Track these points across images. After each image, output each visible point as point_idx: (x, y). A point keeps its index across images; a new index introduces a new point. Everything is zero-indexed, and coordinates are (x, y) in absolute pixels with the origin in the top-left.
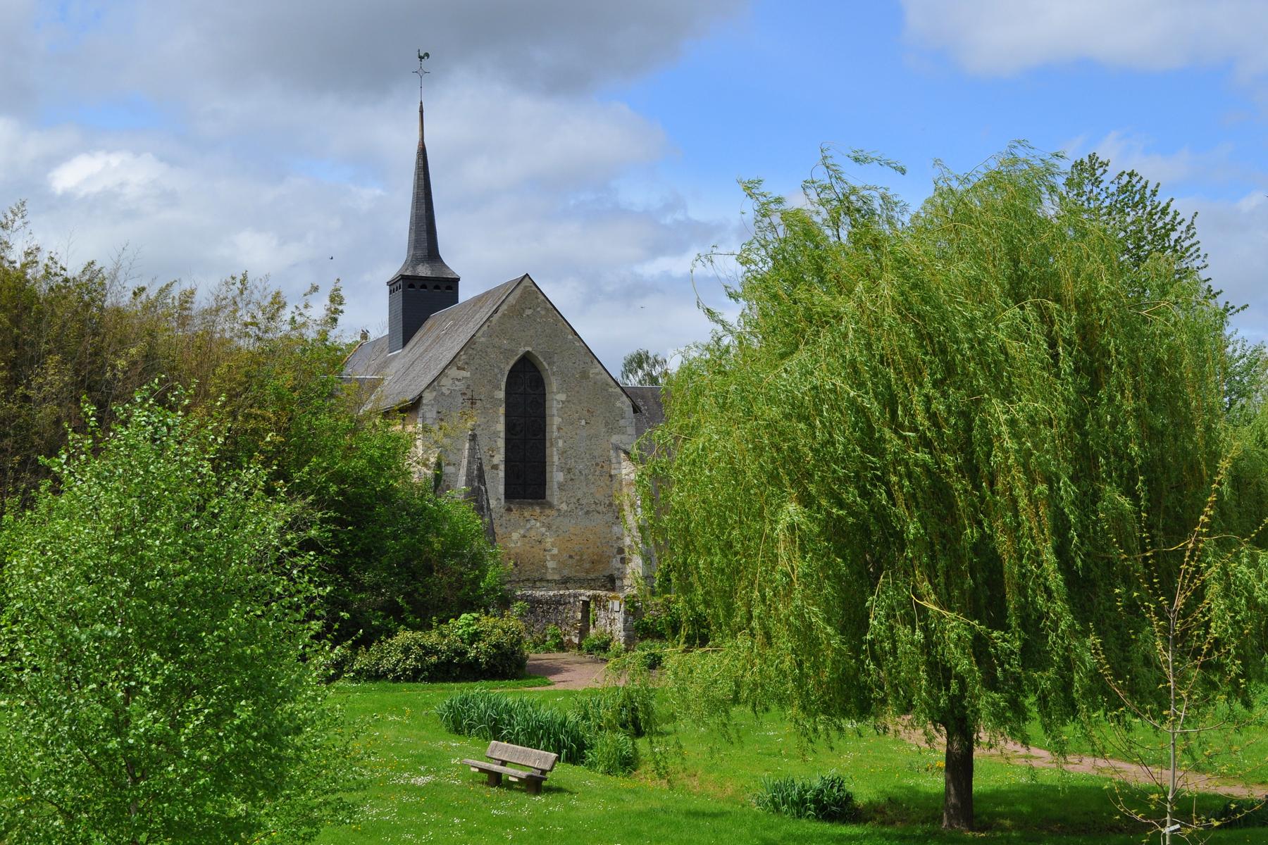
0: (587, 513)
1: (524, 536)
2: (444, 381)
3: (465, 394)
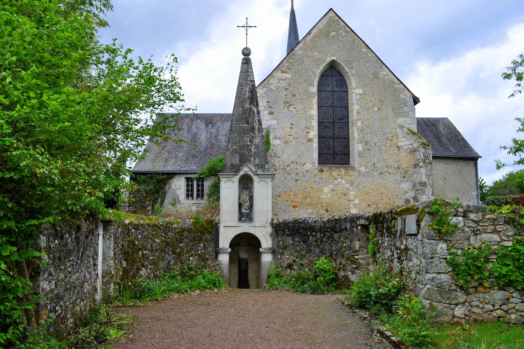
0: (381, 173)
1: (333, 190)
2: (272, 81)
3: (287, 89)
